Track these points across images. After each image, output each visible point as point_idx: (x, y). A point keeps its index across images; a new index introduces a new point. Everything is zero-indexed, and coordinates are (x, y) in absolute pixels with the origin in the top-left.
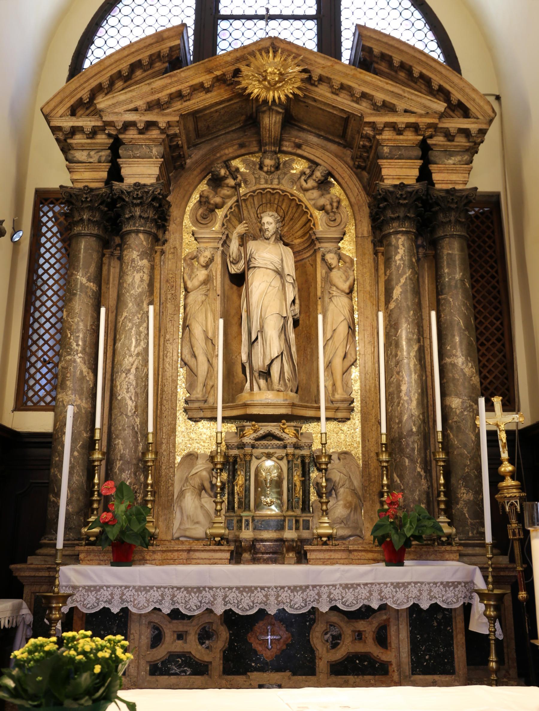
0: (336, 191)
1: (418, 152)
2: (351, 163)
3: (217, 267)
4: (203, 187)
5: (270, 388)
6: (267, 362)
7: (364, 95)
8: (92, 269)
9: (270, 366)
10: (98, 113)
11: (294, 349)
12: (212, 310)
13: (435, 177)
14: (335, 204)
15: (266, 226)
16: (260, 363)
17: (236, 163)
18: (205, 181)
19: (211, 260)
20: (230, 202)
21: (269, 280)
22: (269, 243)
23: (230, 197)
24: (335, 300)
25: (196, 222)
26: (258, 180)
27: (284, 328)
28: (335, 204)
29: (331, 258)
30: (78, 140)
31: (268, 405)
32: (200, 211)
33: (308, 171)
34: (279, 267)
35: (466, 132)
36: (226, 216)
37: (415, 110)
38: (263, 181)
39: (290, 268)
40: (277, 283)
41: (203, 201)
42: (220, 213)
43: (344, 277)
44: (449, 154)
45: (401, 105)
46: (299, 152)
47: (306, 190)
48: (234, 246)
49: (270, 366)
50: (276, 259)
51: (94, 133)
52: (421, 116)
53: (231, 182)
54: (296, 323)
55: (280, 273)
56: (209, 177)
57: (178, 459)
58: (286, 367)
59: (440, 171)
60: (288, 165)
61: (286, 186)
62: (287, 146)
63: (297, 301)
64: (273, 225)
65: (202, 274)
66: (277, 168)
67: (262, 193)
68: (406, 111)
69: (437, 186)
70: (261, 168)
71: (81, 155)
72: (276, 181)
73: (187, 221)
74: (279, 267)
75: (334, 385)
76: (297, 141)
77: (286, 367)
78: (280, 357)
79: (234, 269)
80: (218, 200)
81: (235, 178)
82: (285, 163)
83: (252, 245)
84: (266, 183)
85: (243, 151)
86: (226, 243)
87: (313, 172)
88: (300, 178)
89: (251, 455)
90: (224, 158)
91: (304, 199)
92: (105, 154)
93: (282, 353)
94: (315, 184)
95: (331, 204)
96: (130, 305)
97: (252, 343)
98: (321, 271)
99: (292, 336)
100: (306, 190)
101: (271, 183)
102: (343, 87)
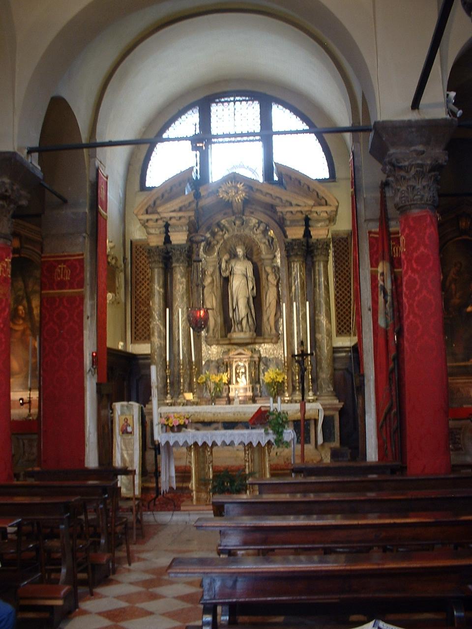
0: (271, 233)
3: (218, 274)
5: (242, 331)
6: (240, 319)
7: (277, 197)
8: (161, 283)
9: (242, 319)
10: (158, 213)
11: (253, 311)
12: (215, 295)
14: (270, 241)
16: (237, 319)
17: (223, 222)
19: (214, 272)
20: (221, 242)
21: (240, 280)
22: (241, 261)
23: (221, 240)
24: (270, 289)
25: (205, 252)
26: (234, 230)
27: (248, 302)
28: (270, 241)
29: (268, 269)
30: (151, 224)
31: (241, 339)
33: (257, 225)
36: (220, 248)
37: (300, 204)
39: (250, 273)
40: (244, 281)
43: (274, 278)
45: (294, 202)
46: (253, 215)
47: (256, 234)
48: (223, 265)
49: (242, 319)
50: (244, 269)
51: (157, 220)
53: (221, 233)
54: (254, 298)
57: (204, 363)
58: (250, 319)
60: (248, 222)
61: (247, 231)
62: (247, 213)
63: (255, 288)
64: (242, 252)
66: (243, 224)
67: (236, 236)
70: (235, 224)
71: (152, 231)
72: (242, 230)
75: (271, 328)
76: (251, 210)
77: (250, 319)
78: (246, 317)
79: (224, 275)
80: (215, 242)
81: (222, 231)
82: (246, 220)
83: (233, 263)
84: (238, 231)
87: (259, 226)
88: (253, 229)
89: (233, 361)
91: (256, 239)
92: (163, 229)
93: (247, 315)
94: (261, 232)
95: (269, 241)
96: (179, 299)
97: (234, 310)
98: (264, 276)
99: (252, 306)
100: (256, 234)
101: (240, 231)
102: (267, 193)
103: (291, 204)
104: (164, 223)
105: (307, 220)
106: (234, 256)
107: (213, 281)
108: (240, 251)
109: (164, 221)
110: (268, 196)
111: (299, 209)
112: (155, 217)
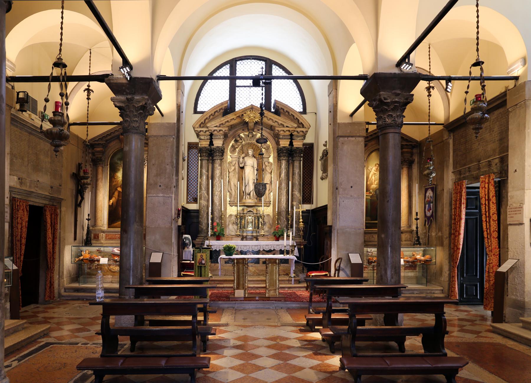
1: (289, 137)
2: (273, 135)
4: (233, 142)
7: (276, 121)
13: (294, 143)
15: (249, 153)
18: (233, 140)
23: (240, 145)
25: (231, 152)
28: (268, 147)
32: (232, 149)
34: (253, 165)
35: (303, 131)
37: (289, 126)
38: (249, 140)
39: (256, 166)
40: (252, 170)
41: (233, 146)
42: (237, 150)
44: (298, 136)
48: (241, 160)
50: (252, 163)
52: (291, 128)
55: (253, 167)
56: (234, 139)
59: (295, 142)
65: (233, 168)
66: (253, 136)
68: (287, 127)
69: (294, 146)
73: (229, 152)
74: (253, 165)
80: (237, 146)
85: (243, 131)
86: (239, 158)
90: (238, 134)
103: (283, 126)
104: (210, 133)
105: (291, 135)
106: (247, 155)
107: (235, 169)
108: (250, 152)
109: (210, 132)
110: (271, 121)
111: (288, 129)
112: (204, 129)
